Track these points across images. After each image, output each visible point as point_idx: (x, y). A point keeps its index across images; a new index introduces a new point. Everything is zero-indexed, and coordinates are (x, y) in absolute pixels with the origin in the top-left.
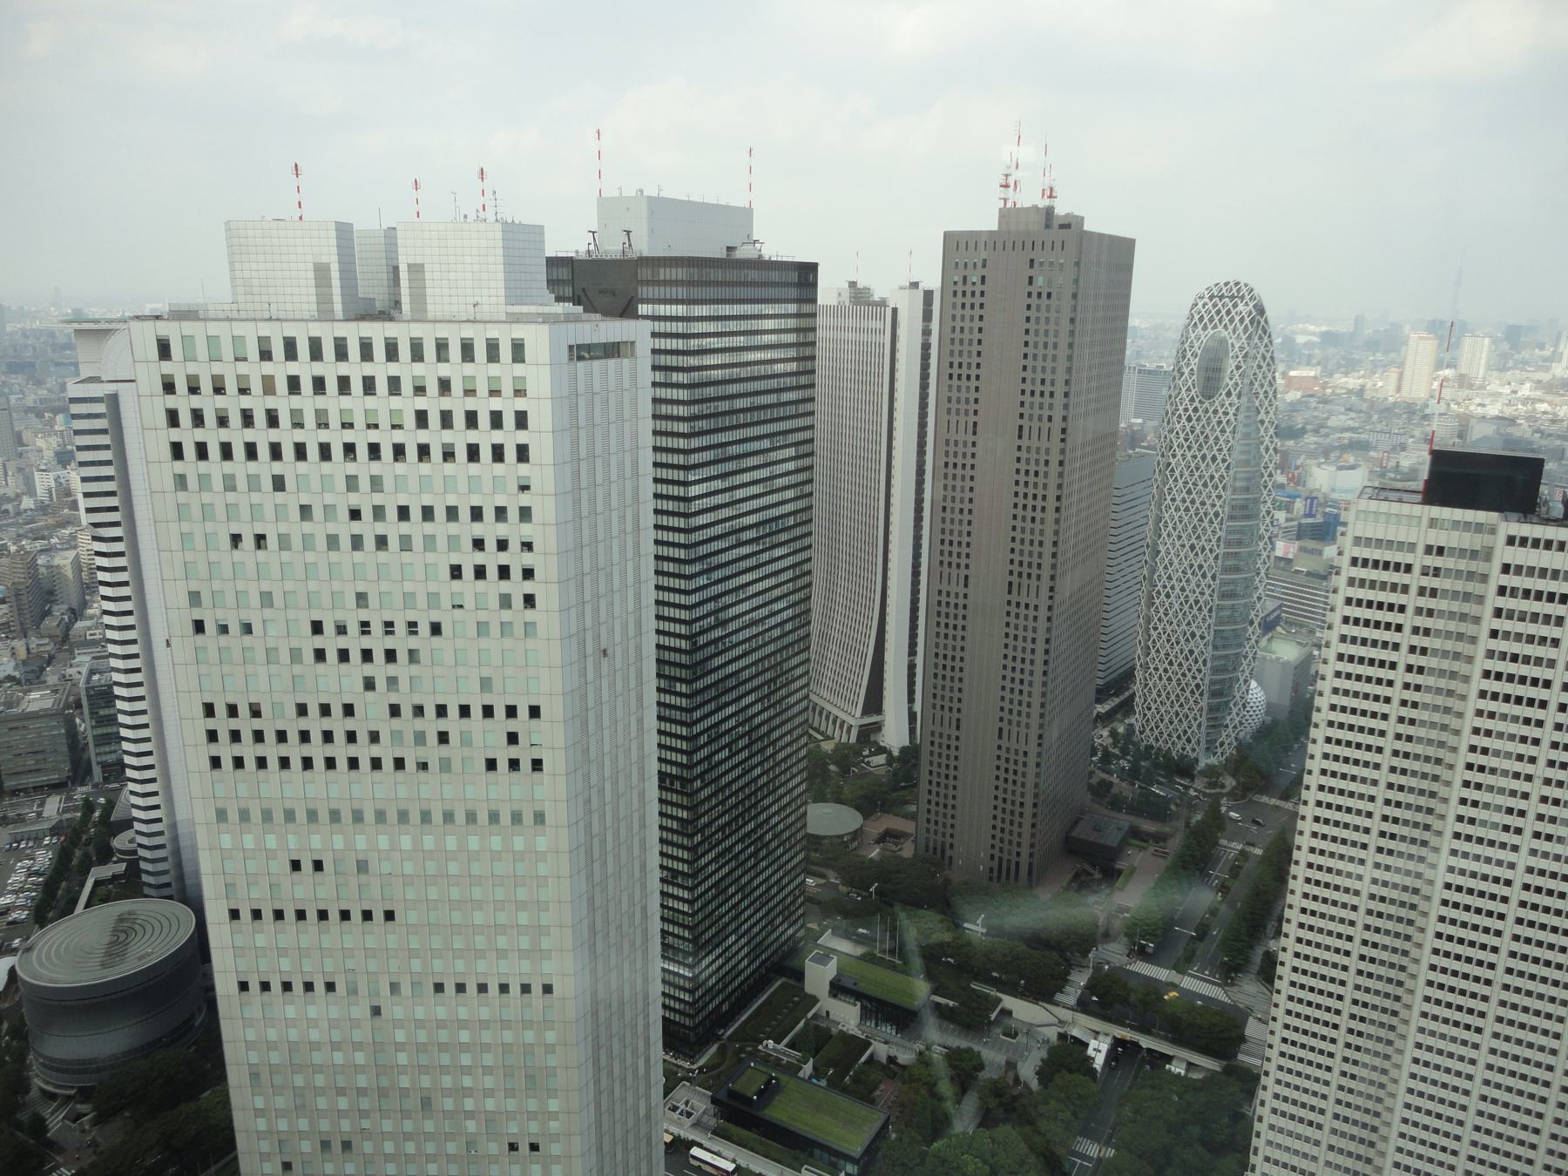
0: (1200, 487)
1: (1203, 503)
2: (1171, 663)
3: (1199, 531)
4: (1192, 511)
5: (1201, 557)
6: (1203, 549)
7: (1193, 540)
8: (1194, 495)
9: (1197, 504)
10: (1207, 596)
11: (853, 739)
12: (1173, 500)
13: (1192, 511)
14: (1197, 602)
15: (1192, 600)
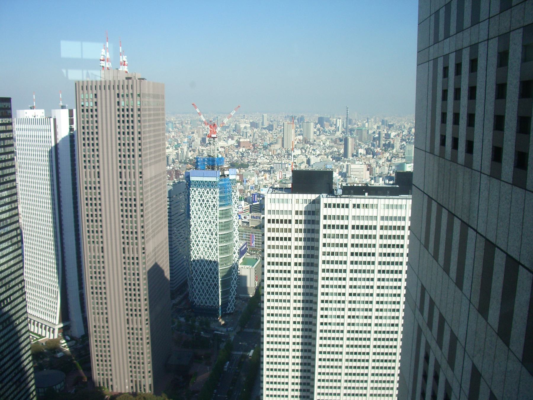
0: (206, 194)
1: (208, 201)
2: (202, 276)
3: (208, 214)
4: (204, 205)
5: (210, 226)
6: (210, 222)
7: (206, 218)
8: (203, 198)
9: (205, 202)
10: (214, 243)
11: (56, 337)
12: (195, 201)
13: (204, 205)
14: (210, 246)
15: (208, 246)
